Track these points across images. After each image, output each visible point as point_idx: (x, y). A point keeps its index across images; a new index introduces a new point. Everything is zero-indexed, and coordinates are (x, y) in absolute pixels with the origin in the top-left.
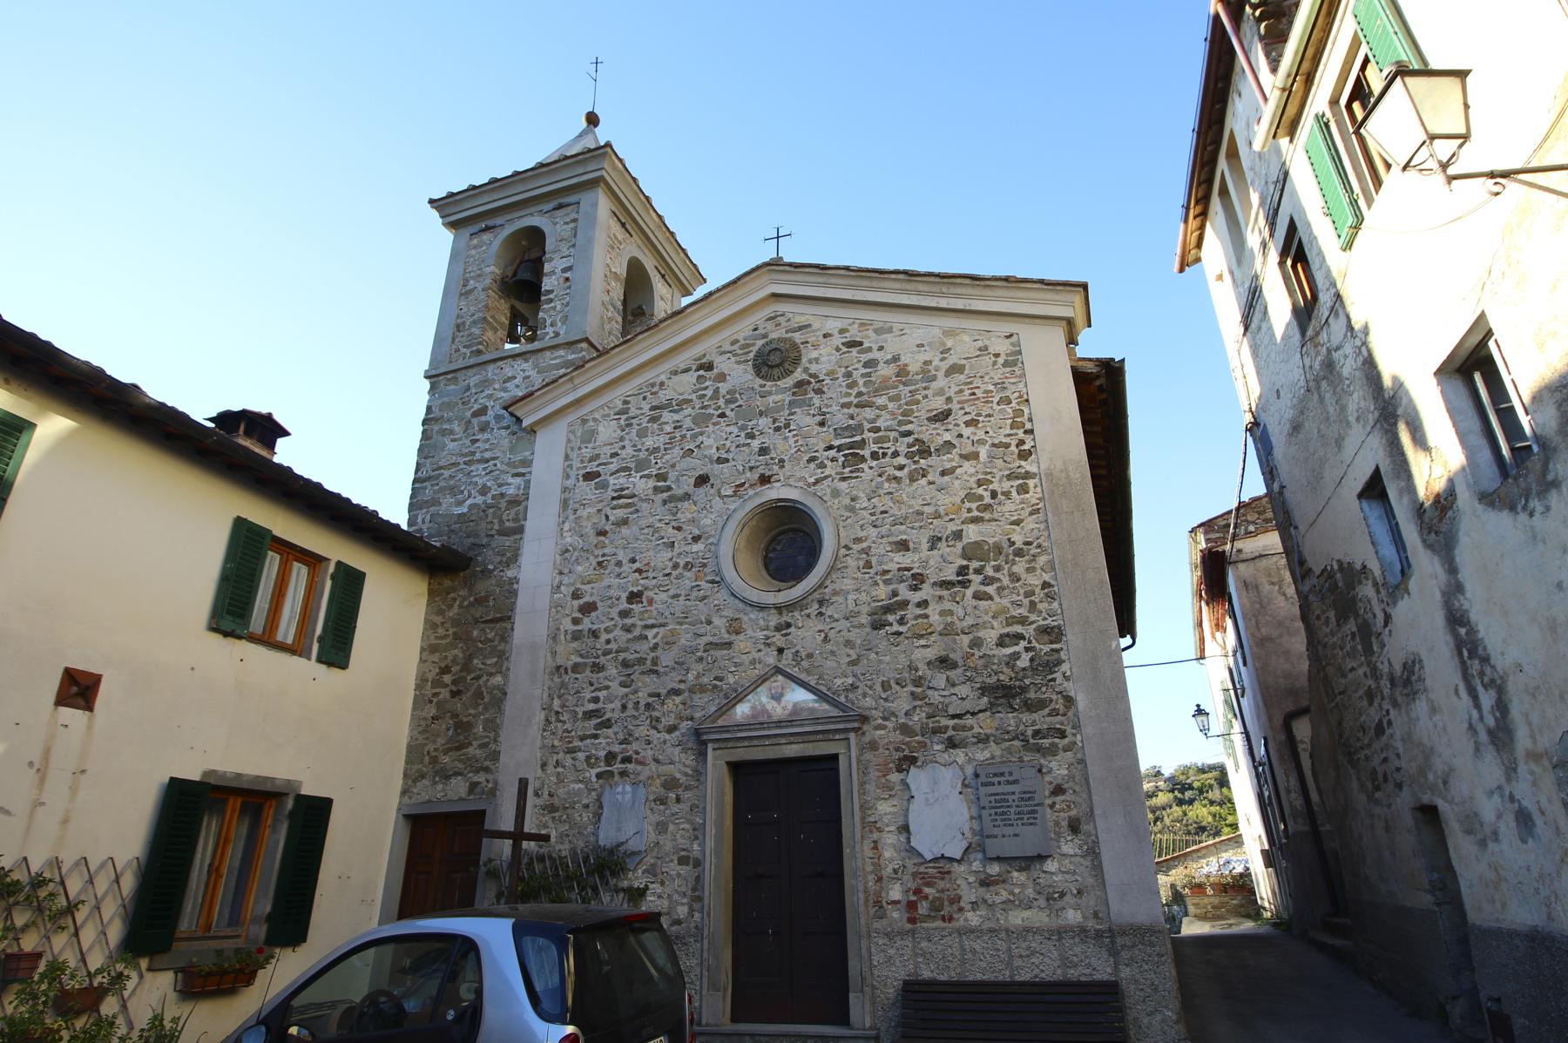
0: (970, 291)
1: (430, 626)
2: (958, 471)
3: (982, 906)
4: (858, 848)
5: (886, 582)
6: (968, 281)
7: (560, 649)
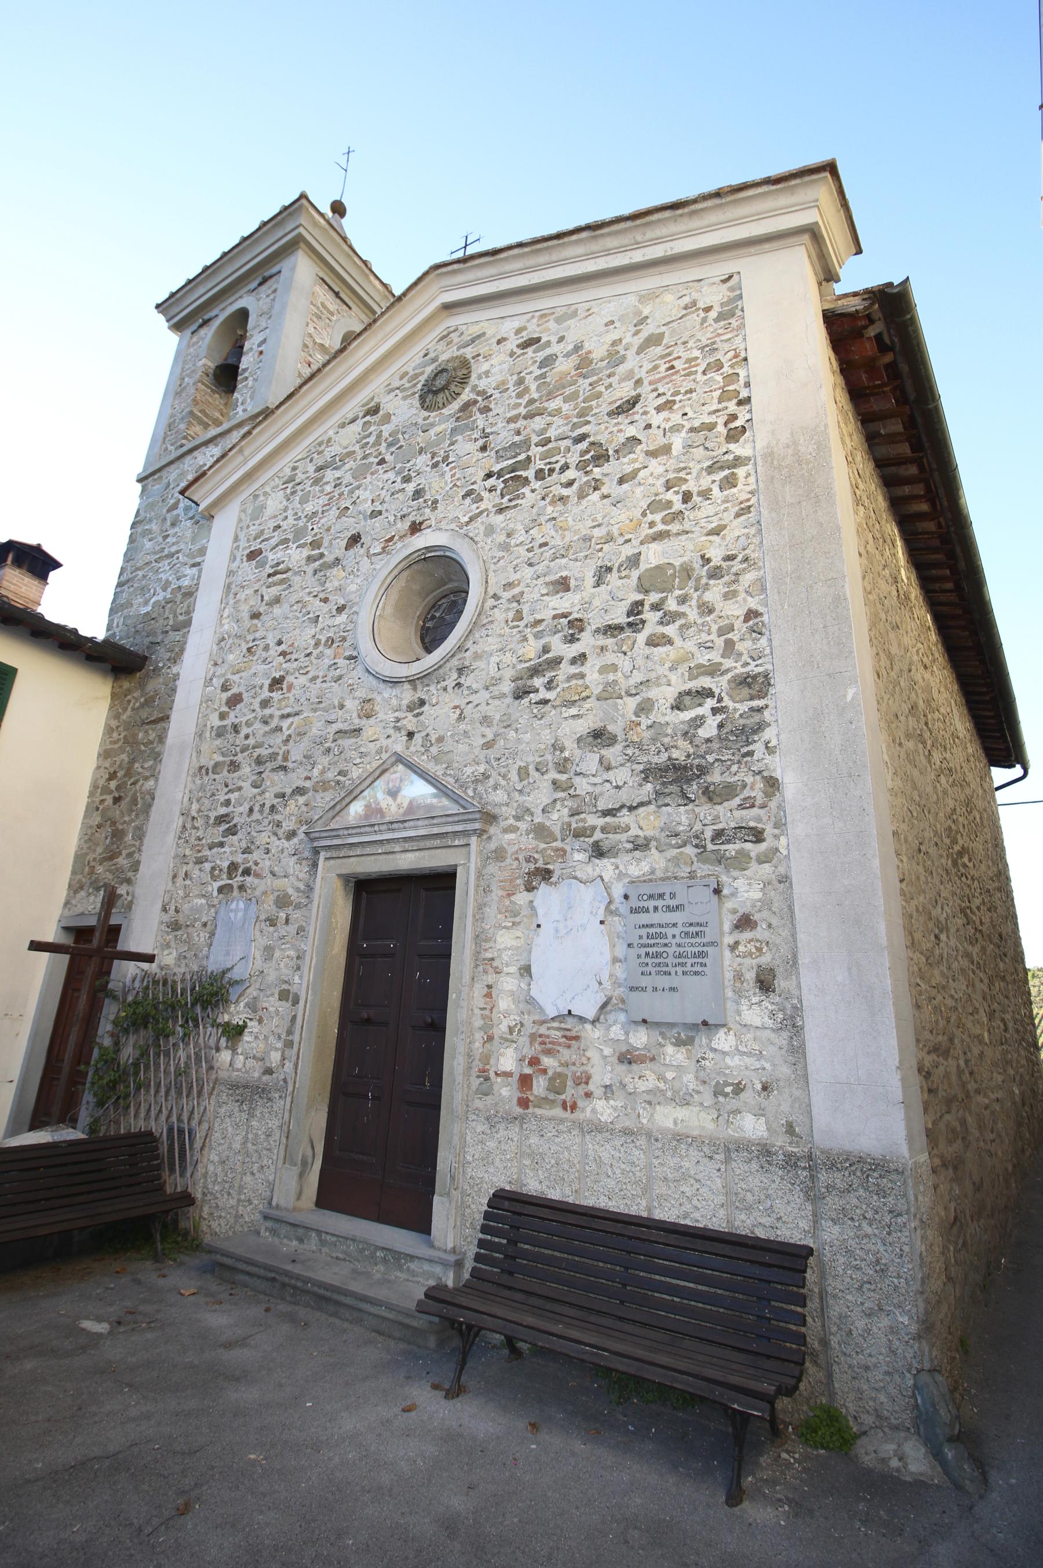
0: (673, 228)
1: (109, 730)
2: (642, 474)
4: (465, 990)
5: (538, 636)
6: (667, 214)
7: (205, 747)
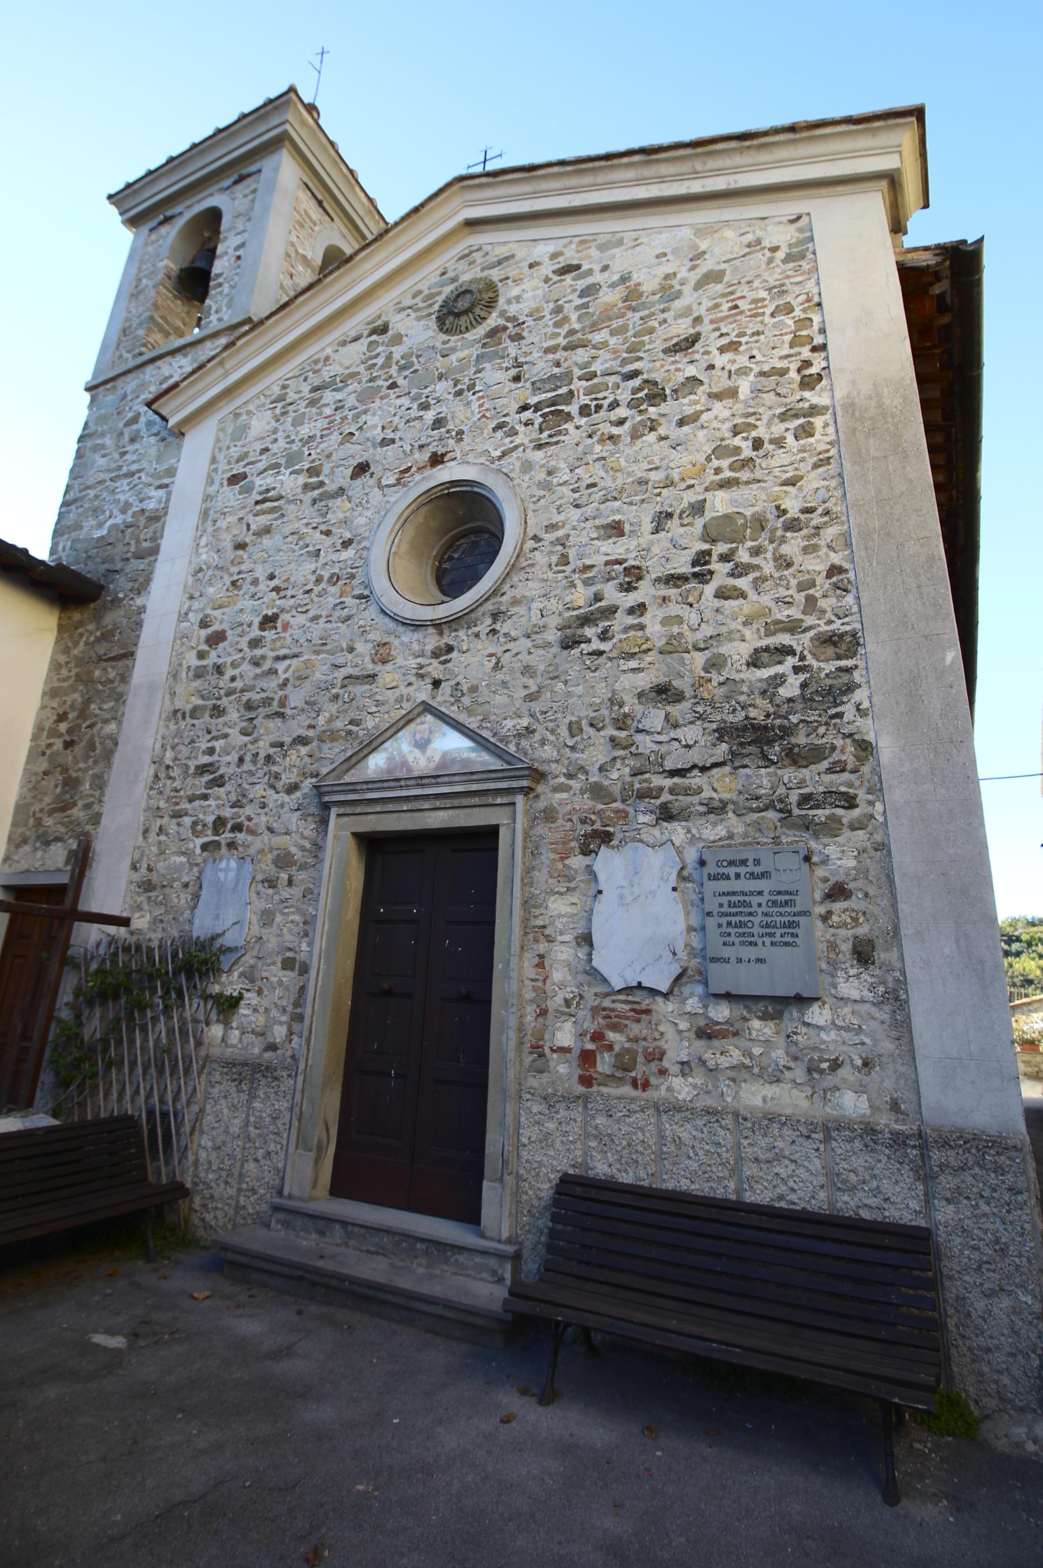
0: (737, 160)
1: (55, 666)
2: (704, 417)
3: (698, 1071)
4: (514, 962)
5: (587, 583)
6: (733, 144)
7: (180, 689)
